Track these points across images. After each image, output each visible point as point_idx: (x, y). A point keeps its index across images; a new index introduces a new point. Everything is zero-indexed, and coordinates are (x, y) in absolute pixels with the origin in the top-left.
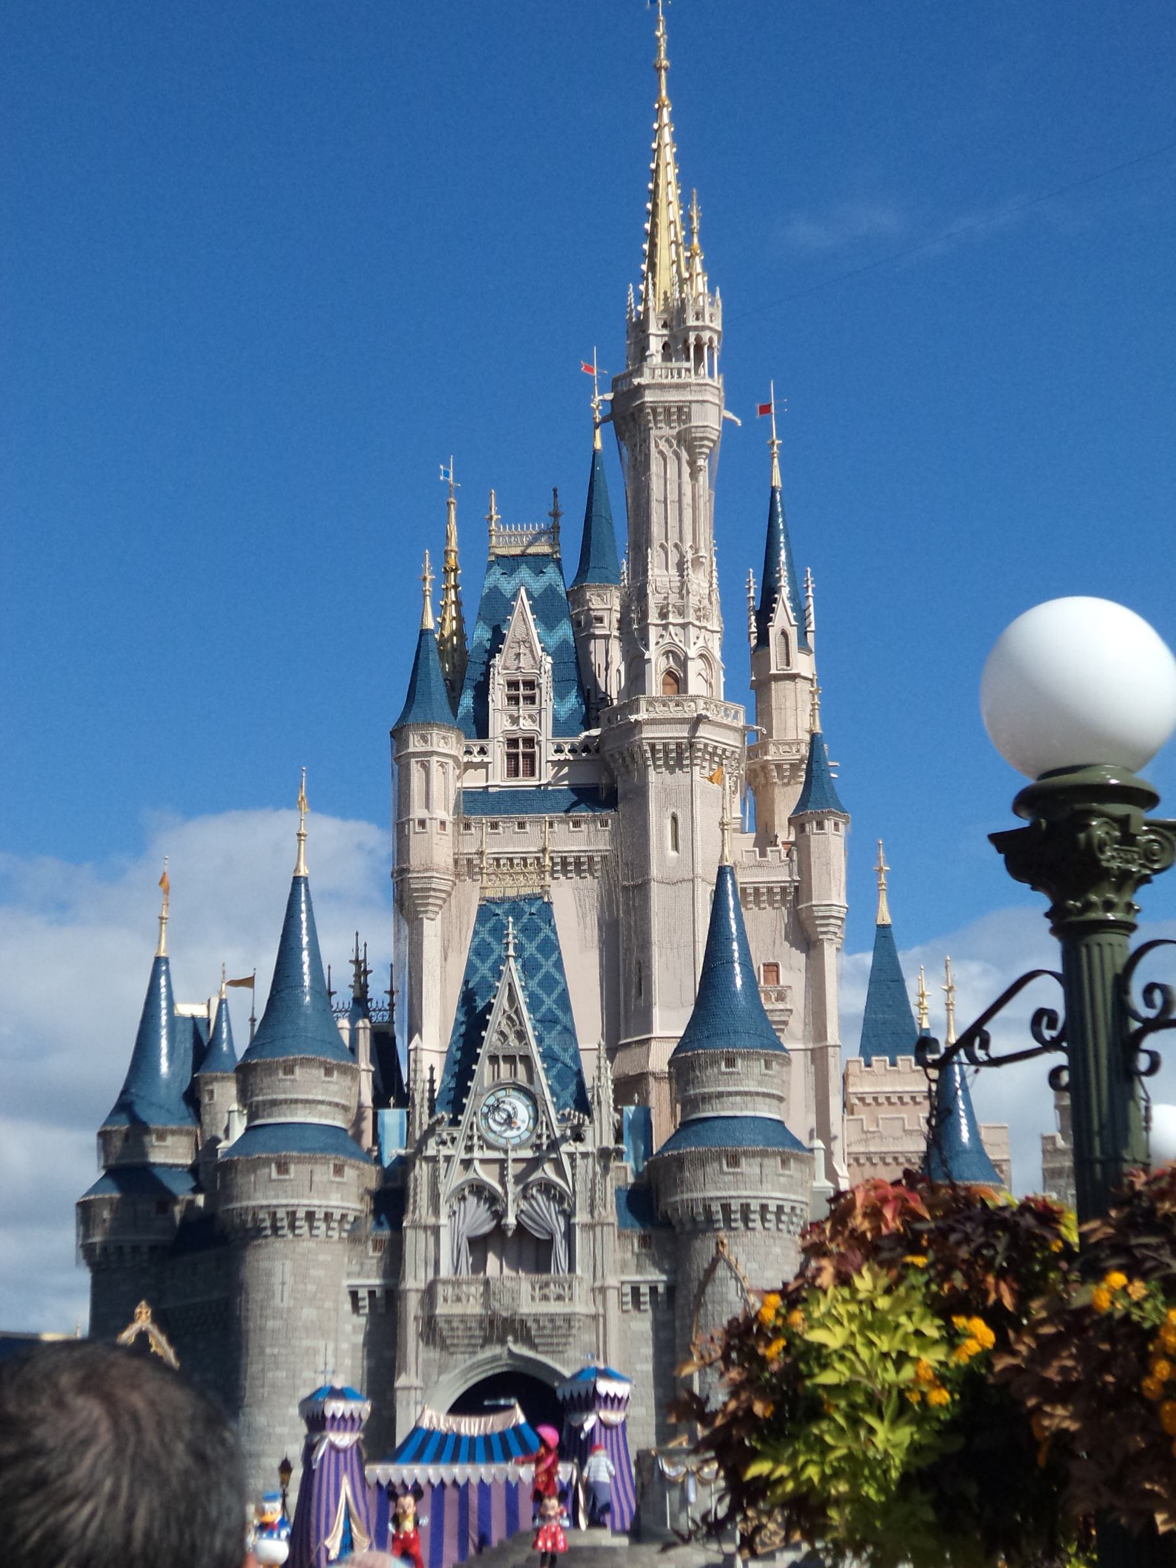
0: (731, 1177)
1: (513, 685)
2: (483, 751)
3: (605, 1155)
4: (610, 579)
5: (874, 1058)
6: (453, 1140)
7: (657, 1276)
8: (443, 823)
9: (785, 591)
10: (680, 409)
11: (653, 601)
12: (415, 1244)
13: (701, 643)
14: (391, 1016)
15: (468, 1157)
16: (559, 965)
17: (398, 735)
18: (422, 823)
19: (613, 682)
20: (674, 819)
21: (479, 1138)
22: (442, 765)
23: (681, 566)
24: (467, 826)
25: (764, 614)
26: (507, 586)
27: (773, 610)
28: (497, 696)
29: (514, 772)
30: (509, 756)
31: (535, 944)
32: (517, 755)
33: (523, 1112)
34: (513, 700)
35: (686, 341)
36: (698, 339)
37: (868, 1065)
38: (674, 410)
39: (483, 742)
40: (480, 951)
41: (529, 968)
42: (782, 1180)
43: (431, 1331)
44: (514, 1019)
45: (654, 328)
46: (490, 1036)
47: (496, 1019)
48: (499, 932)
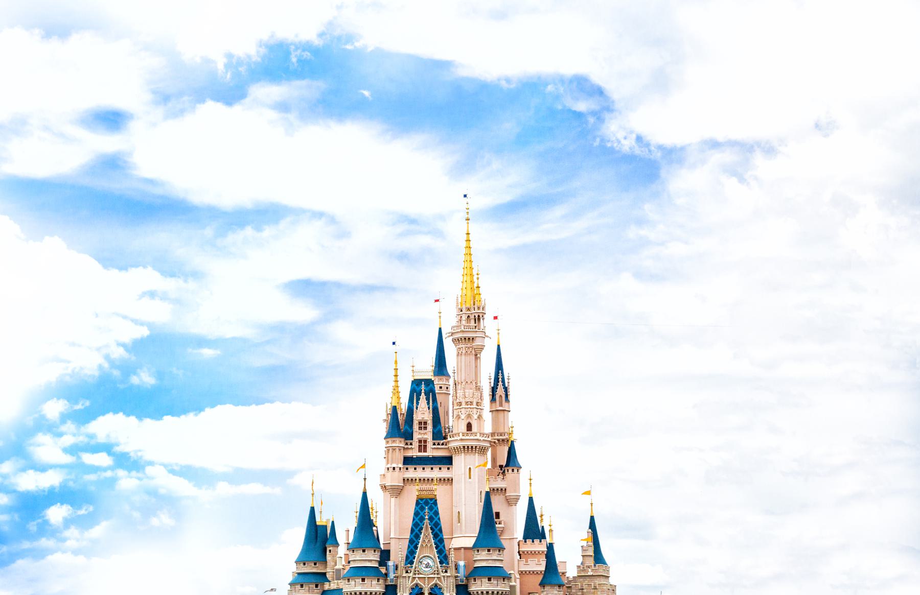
0: (489, 584)
1: (420, 423)
2: (411, 444)
5: (527, 540)
6: (411, 571)
8: (400, 468)
9: (500, 382)
10: (473, 338)
13: (478, 413)
14: (376, 520)
15: (414, 576)
16: (439, 519)
18: (394, 468)
20: (470, 468)
21: (418, 571)
22: (400, 450)
24: (407, 469)
26: (418, 389)
27: (497, 388)
28: (416, 427)
29: (420, 451)
30: (419, 445)
31: (432, 515)
32: (421, 445)
34: (420, 428)
35: (475, 316)
36: (479, 316)
37: (525, 542)
38: (471, 339)
39: (411, 441)
40: (416, 514)
41: (431, 519)
42: (503, 585)
47: (422, 536)
48: (422, 509)
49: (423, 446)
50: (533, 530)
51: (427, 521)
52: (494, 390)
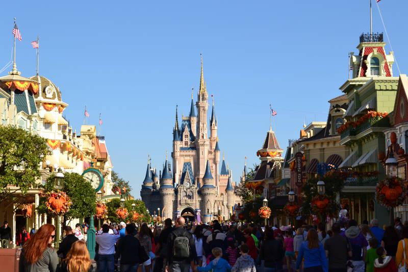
3: (196, 188)
4: (194, 116)
7: (200, 199)
11: (200, 128)
12: (179, 196)
17: (174, 141)
19: (195, 134)
23: (203, 124)
25: (211, 122)
33: (188, 184)
40: (184, 168)
43: (180, 204)
44: (188, 175)
45: (201, 96)
46: (186, 177)
48: (186, 166)
49: (186, 143)
50: (224, 171)
51: (188, 170)
52: (211, 122)
